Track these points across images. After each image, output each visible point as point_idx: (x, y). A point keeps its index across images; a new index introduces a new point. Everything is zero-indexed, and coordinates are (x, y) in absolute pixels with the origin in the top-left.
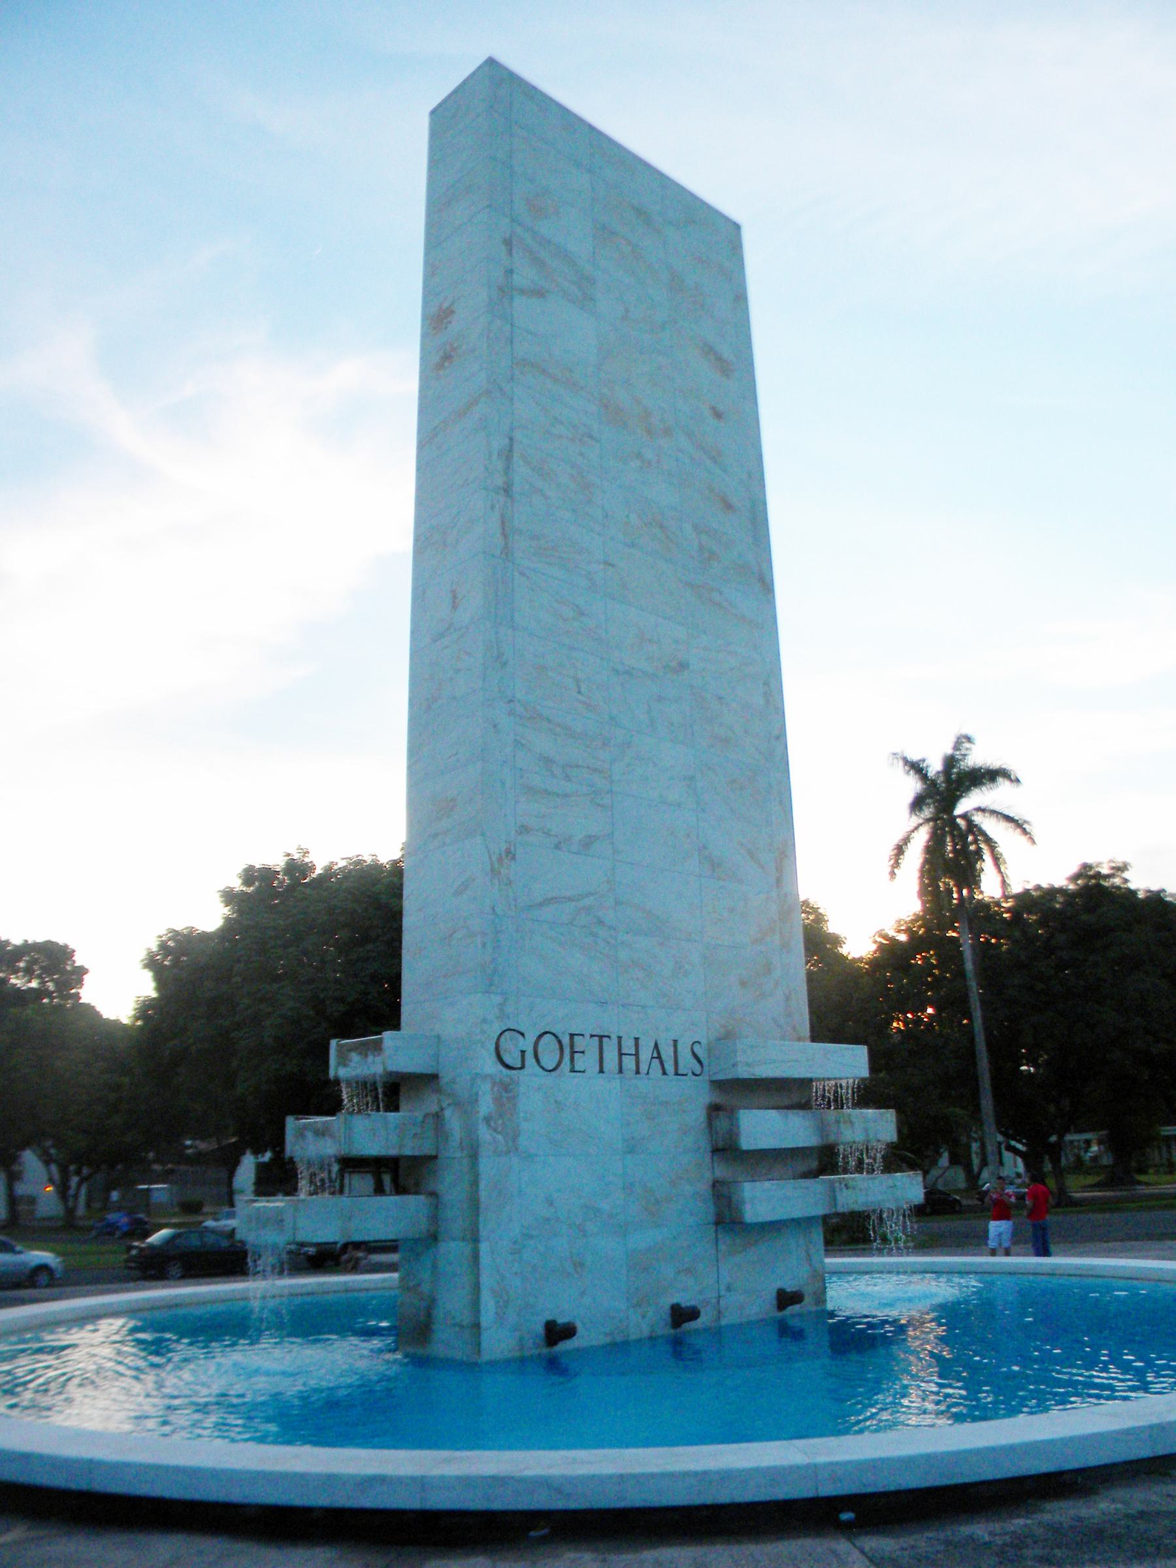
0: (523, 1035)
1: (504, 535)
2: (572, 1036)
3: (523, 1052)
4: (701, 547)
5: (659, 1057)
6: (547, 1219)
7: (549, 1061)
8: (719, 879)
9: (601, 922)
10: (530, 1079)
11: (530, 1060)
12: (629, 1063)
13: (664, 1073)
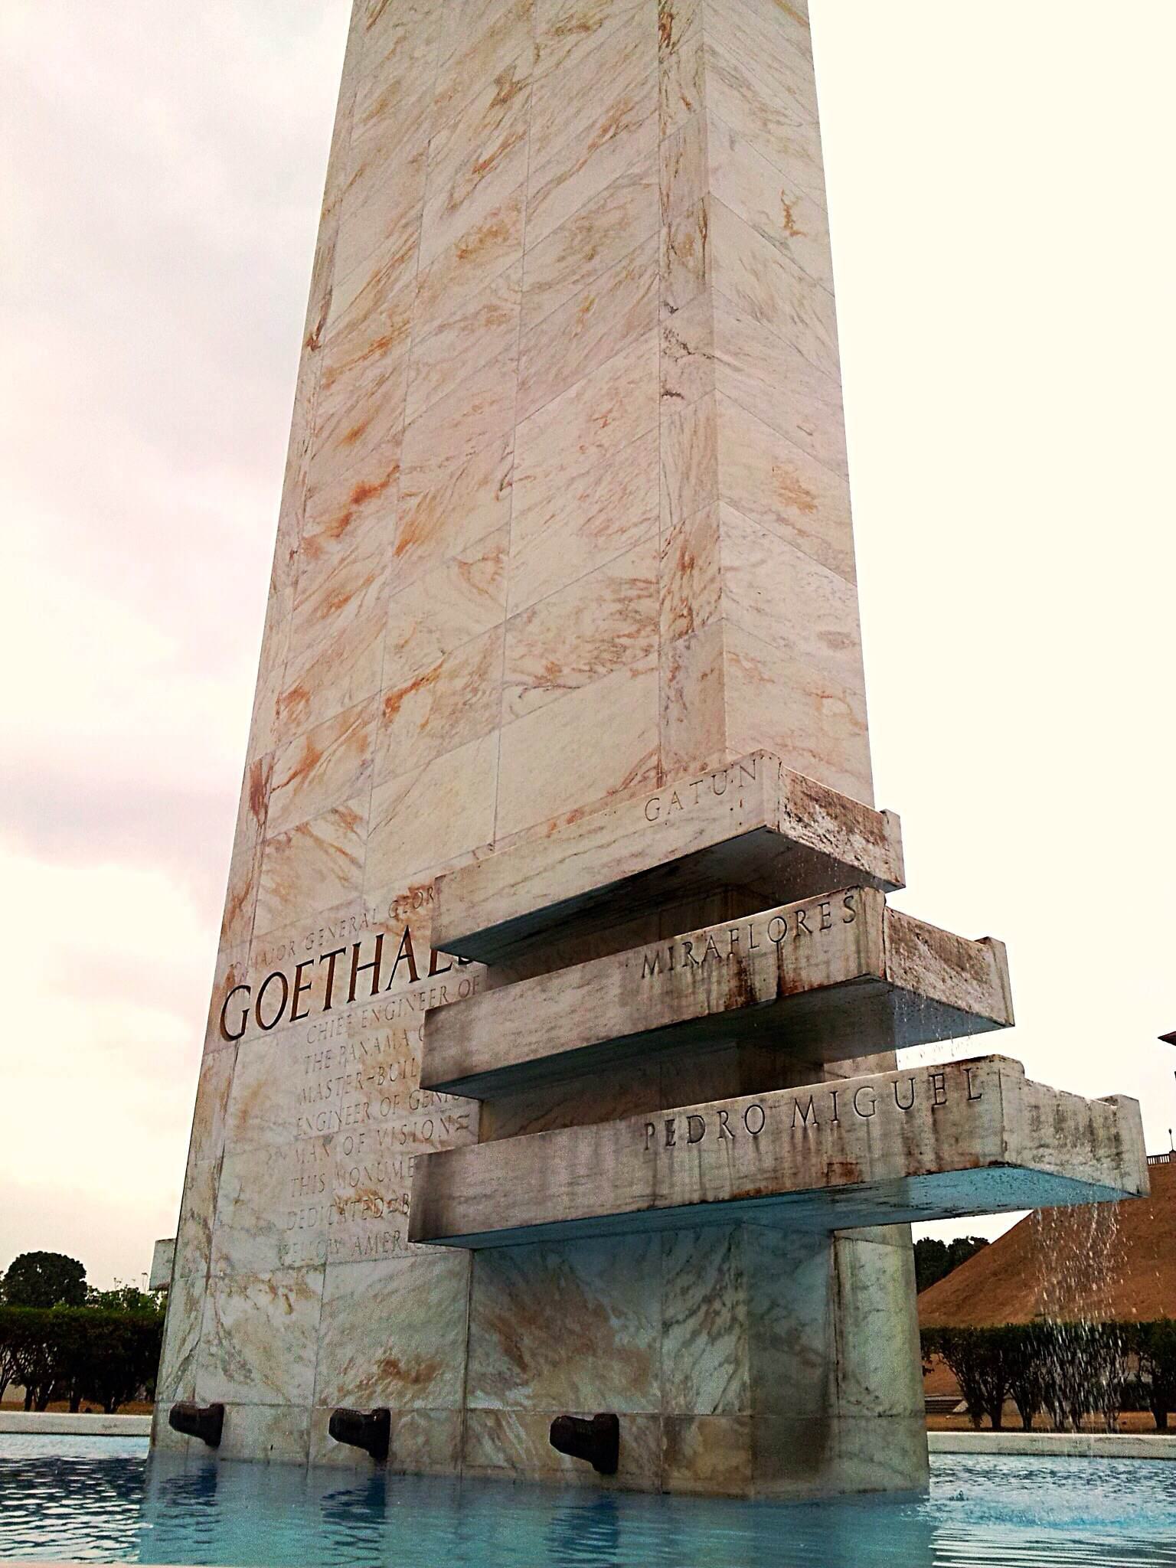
0: (248, 989)
2: (299, 967)
3: (246, 1012)
5: (410, 955)
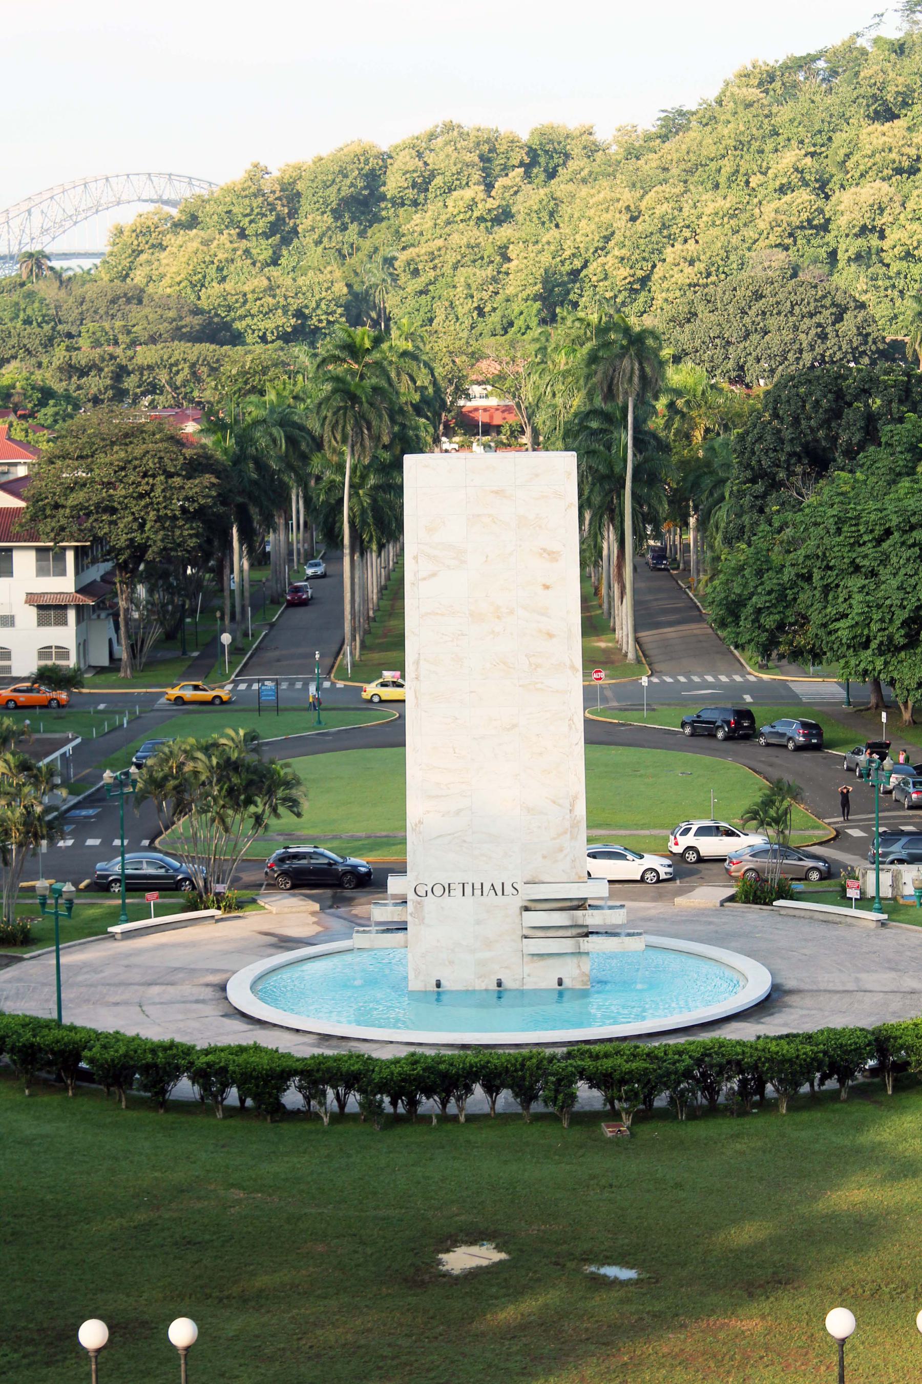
1: (416, 697)
4: (530, 664)
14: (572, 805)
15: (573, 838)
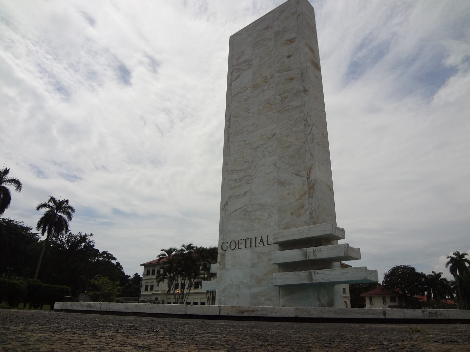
1: (228, 137)
2: (239, 241)
5: (262, 241)
6: (230, 284)
7: (233, 247)
8: (285, 186)
9: (247, 211)
10: (229, 252)
11: (229, 248)
12: (253, 244)
13: (264, 245)
14: (309, 174)
15: (311, 196)
